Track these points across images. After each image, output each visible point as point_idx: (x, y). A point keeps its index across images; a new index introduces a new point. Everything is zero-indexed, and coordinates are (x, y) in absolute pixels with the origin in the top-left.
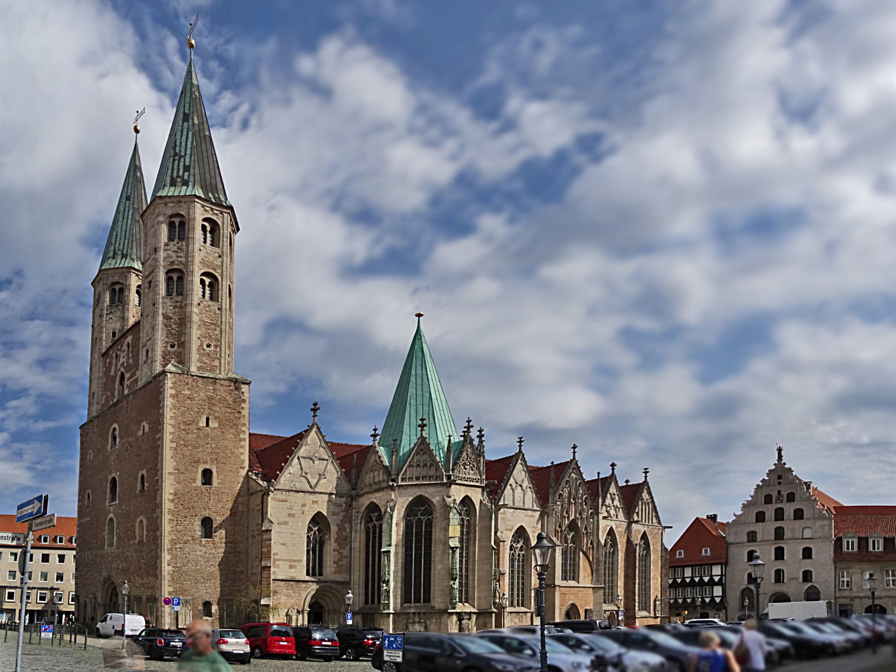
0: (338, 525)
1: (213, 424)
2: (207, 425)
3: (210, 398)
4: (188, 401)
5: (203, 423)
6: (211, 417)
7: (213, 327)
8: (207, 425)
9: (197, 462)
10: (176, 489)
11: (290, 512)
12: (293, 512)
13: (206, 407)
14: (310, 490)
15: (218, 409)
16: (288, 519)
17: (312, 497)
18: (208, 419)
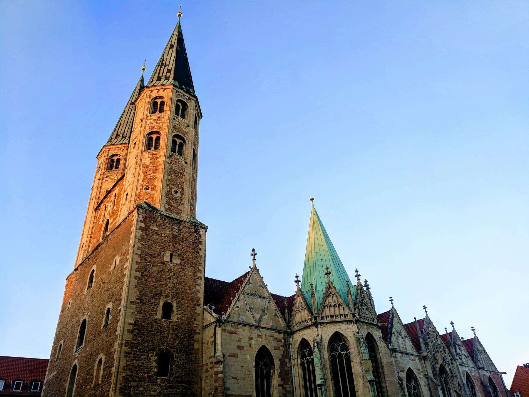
0: (280, 360)
1: (176, 261)
2: (171, 261)
3: (174, 237)
4: (155, 236)
5: (167, 258)
6: (174, 254)
7: (180, 175)
8: (171, 261)
9: (160, 294)
10: (137, 320)
11: (239, 344)
12: (242, 344)
13: (171, 244)
14: (255, 324)
15: (180, 247)
16: (238, 352)
17: (257, 332)
18: (171, 255)
